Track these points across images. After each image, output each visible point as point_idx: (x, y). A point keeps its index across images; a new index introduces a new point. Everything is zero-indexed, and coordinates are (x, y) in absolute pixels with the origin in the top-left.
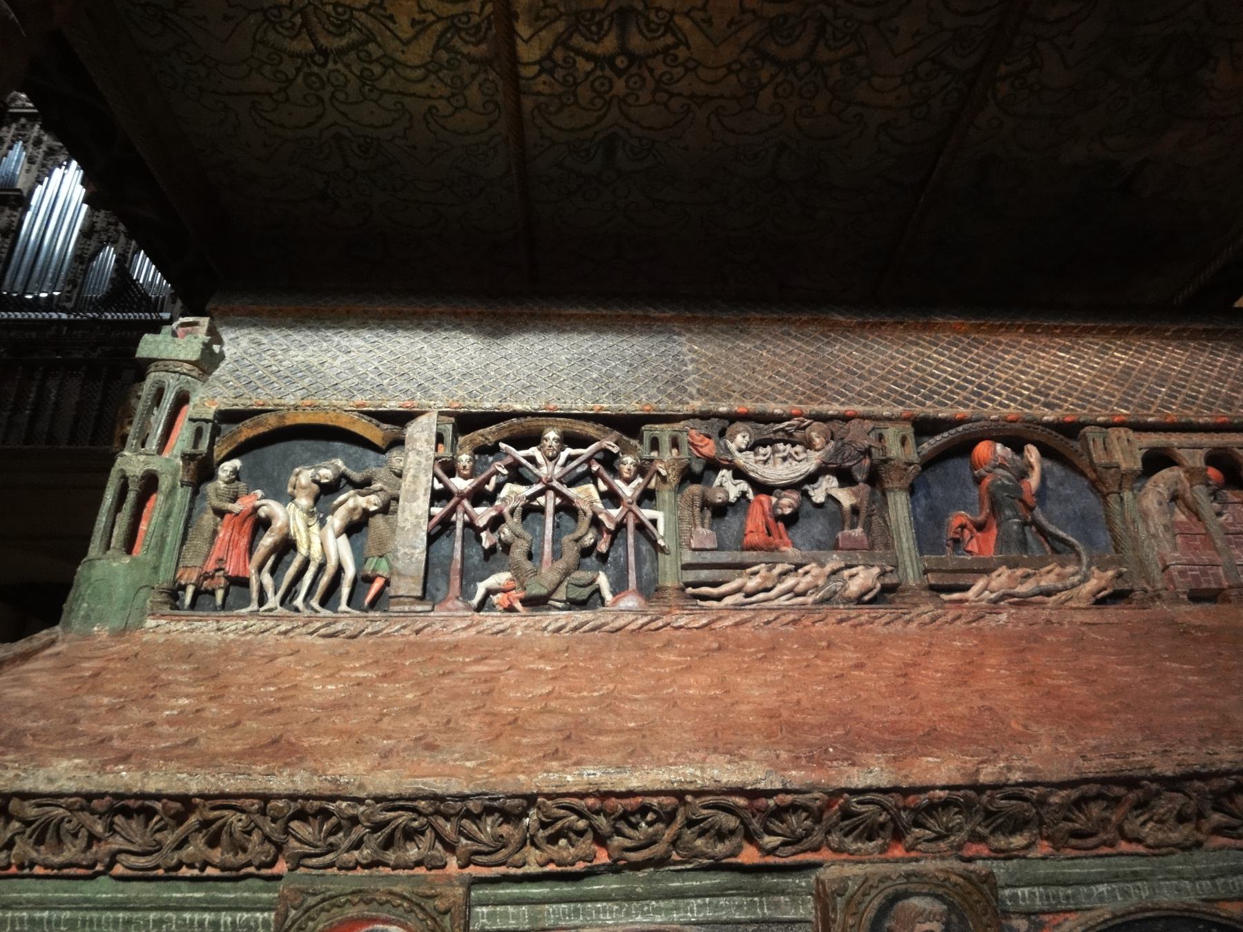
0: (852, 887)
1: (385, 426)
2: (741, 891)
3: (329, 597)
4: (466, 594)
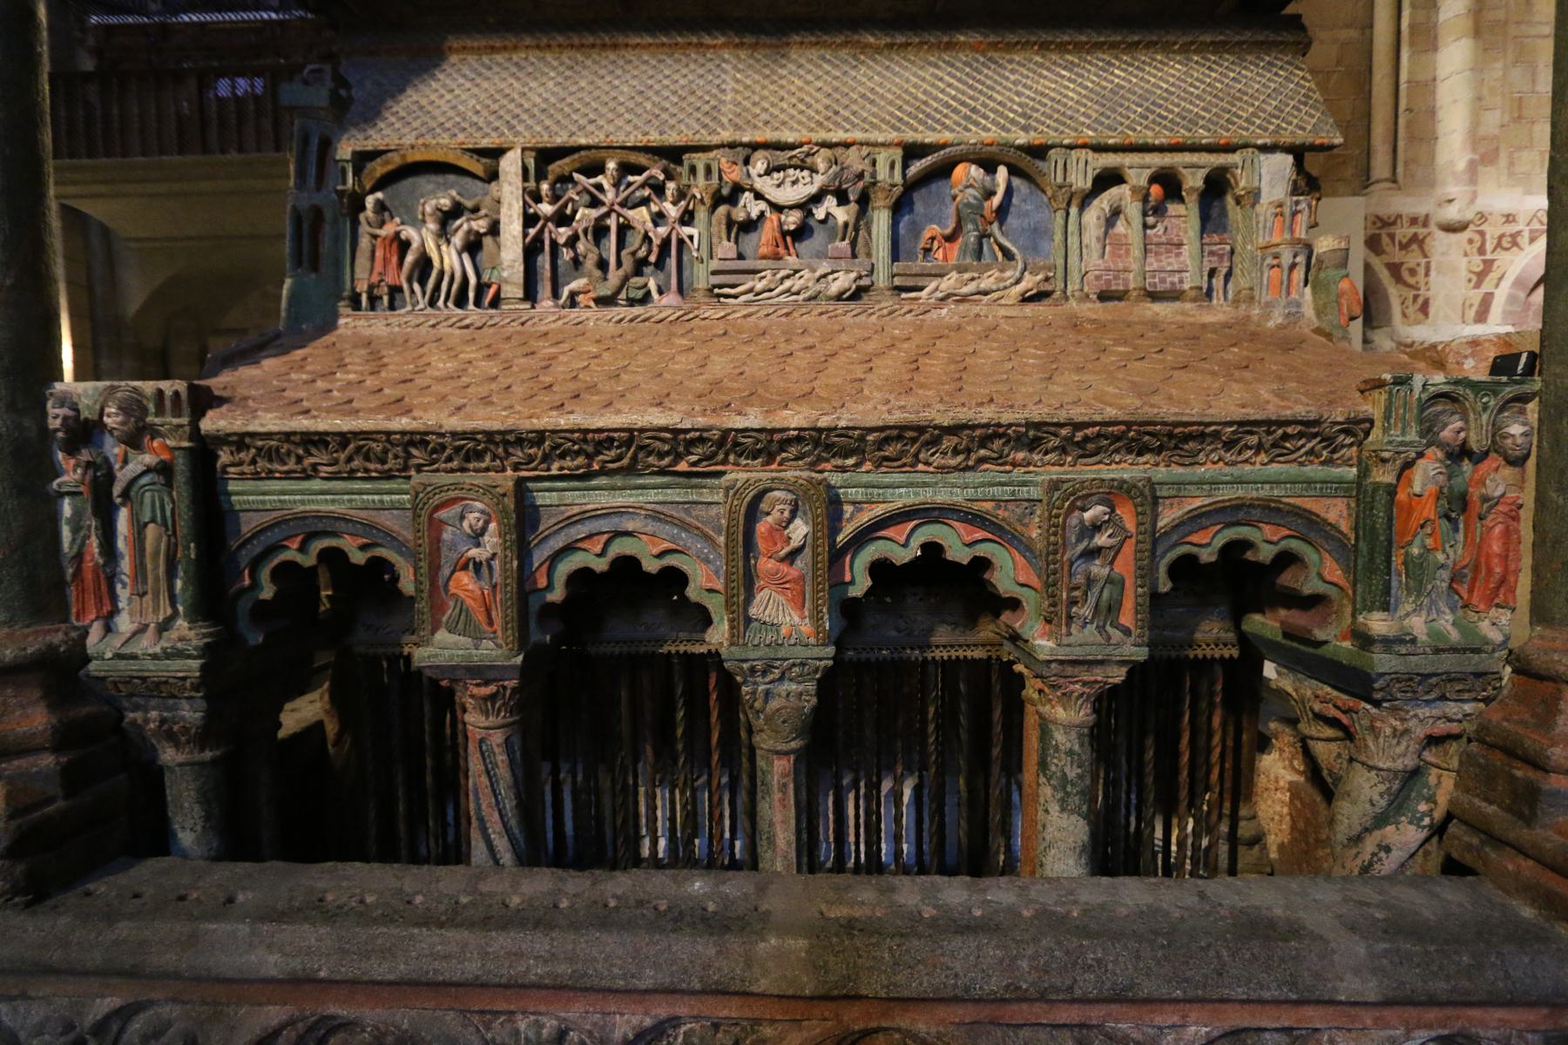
0: (739, 484)
1: (484, 160)
4: (556, 295)
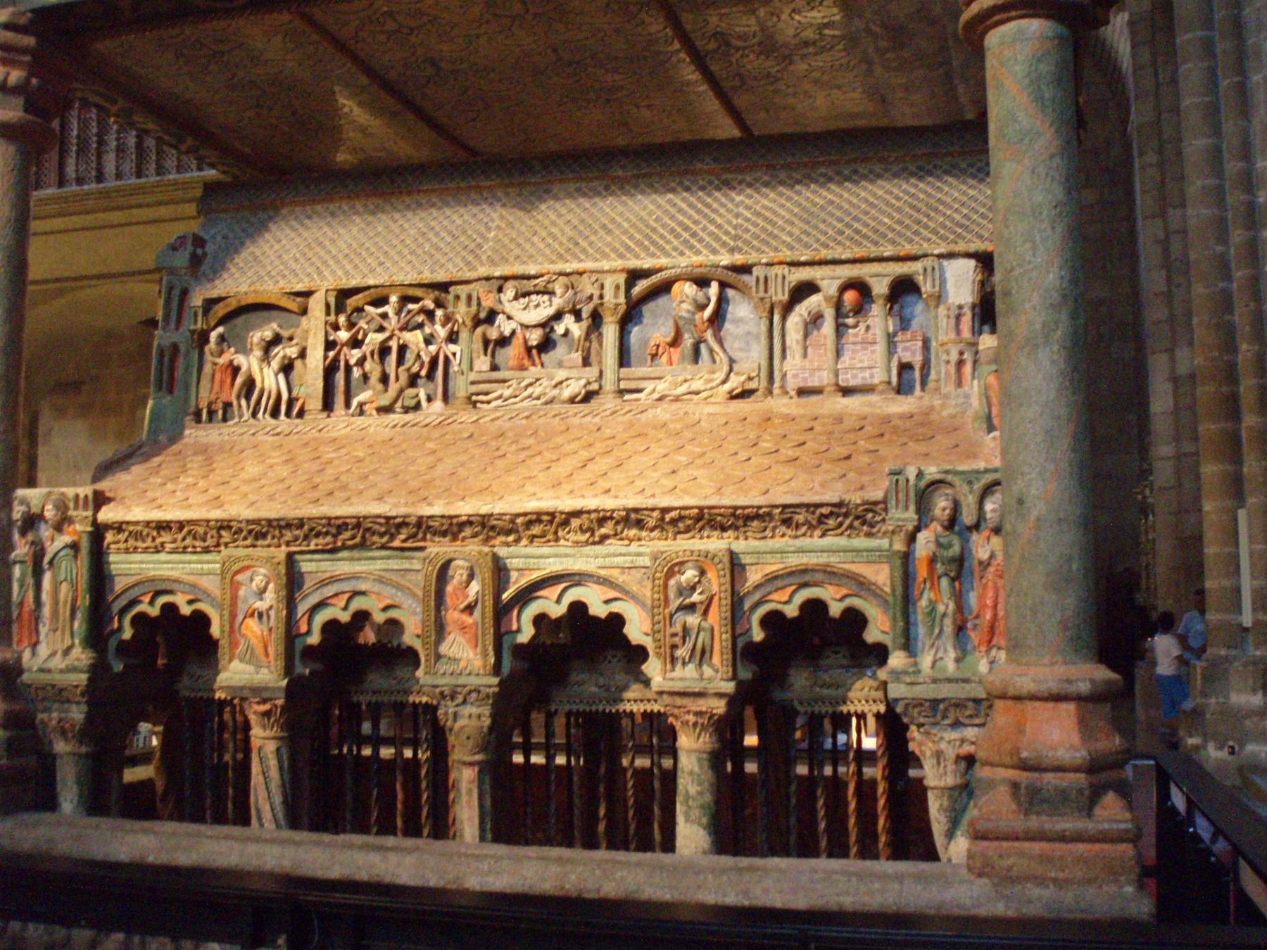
1: (299, 299)
2: (396, 557)
4: (348, 405)
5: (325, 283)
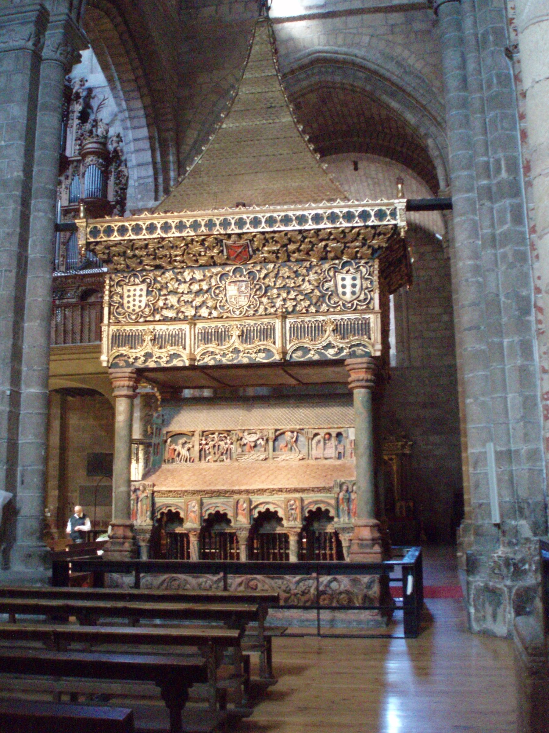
3: (186, 461)
4: (205, 459)
5: (199, 429)
